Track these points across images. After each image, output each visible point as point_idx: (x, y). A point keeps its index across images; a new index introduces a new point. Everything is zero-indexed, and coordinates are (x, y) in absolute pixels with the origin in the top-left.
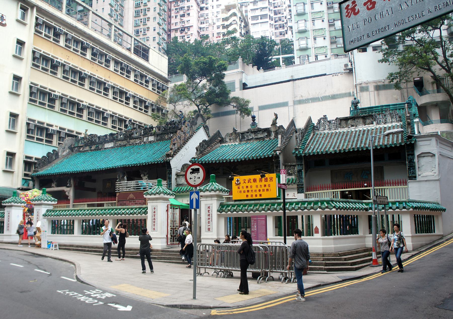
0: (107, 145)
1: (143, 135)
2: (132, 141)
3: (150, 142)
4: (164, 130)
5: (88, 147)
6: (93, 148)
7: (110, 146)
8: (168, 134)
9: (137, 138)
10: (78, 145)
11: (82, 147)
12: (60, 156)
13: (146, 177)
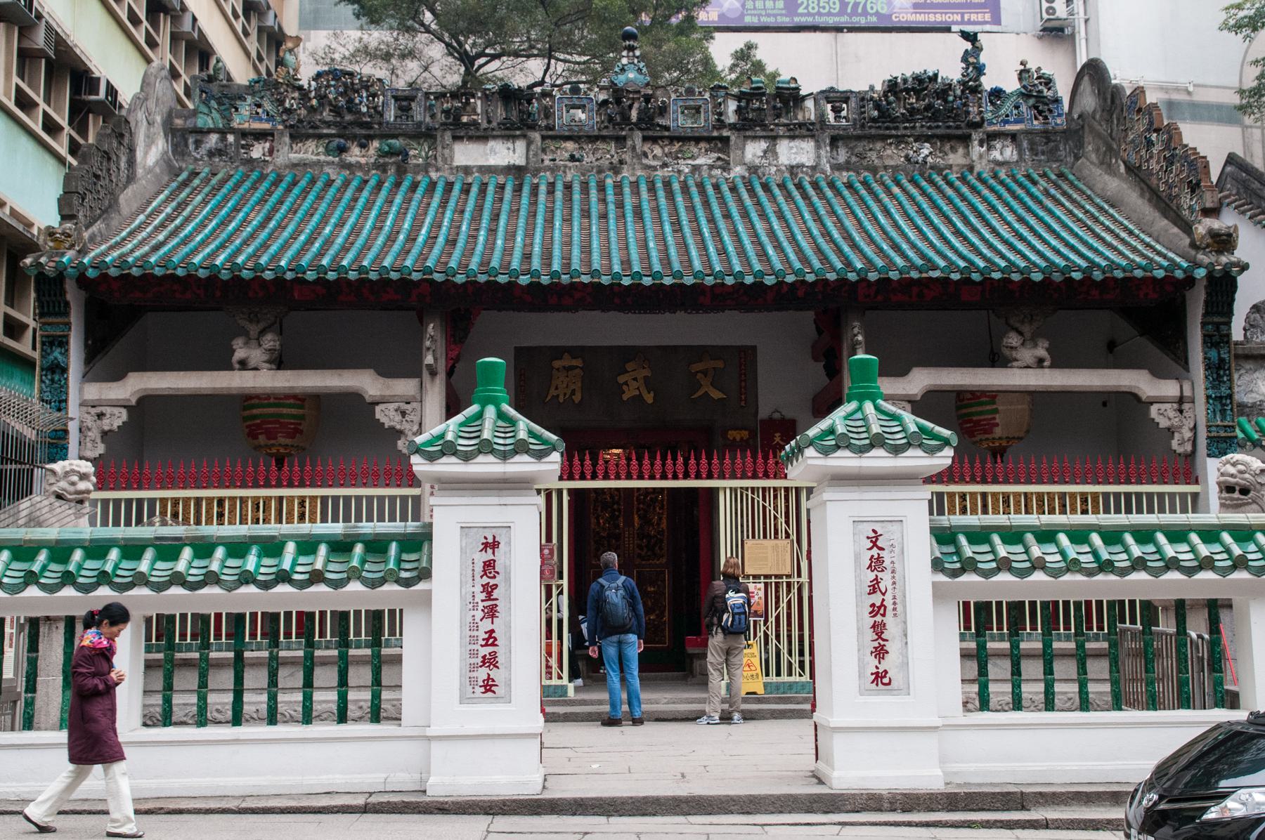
0: (467, 154)
1: (733, 127)
2: (658, 151)
3: (793, 169)
4: (873, 120)
5: (311, 145)
6: (355, 155)
7: (493, 161)
8: (900, 140)
9: (697, 140)
10: (230, 120)
11: (261, 136)
12: (140, 171)
13: (1041, 352)
